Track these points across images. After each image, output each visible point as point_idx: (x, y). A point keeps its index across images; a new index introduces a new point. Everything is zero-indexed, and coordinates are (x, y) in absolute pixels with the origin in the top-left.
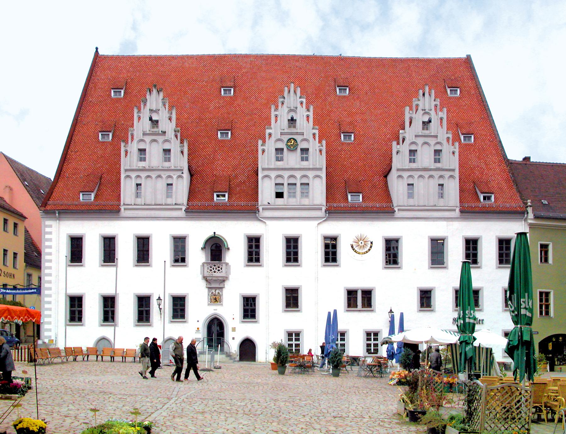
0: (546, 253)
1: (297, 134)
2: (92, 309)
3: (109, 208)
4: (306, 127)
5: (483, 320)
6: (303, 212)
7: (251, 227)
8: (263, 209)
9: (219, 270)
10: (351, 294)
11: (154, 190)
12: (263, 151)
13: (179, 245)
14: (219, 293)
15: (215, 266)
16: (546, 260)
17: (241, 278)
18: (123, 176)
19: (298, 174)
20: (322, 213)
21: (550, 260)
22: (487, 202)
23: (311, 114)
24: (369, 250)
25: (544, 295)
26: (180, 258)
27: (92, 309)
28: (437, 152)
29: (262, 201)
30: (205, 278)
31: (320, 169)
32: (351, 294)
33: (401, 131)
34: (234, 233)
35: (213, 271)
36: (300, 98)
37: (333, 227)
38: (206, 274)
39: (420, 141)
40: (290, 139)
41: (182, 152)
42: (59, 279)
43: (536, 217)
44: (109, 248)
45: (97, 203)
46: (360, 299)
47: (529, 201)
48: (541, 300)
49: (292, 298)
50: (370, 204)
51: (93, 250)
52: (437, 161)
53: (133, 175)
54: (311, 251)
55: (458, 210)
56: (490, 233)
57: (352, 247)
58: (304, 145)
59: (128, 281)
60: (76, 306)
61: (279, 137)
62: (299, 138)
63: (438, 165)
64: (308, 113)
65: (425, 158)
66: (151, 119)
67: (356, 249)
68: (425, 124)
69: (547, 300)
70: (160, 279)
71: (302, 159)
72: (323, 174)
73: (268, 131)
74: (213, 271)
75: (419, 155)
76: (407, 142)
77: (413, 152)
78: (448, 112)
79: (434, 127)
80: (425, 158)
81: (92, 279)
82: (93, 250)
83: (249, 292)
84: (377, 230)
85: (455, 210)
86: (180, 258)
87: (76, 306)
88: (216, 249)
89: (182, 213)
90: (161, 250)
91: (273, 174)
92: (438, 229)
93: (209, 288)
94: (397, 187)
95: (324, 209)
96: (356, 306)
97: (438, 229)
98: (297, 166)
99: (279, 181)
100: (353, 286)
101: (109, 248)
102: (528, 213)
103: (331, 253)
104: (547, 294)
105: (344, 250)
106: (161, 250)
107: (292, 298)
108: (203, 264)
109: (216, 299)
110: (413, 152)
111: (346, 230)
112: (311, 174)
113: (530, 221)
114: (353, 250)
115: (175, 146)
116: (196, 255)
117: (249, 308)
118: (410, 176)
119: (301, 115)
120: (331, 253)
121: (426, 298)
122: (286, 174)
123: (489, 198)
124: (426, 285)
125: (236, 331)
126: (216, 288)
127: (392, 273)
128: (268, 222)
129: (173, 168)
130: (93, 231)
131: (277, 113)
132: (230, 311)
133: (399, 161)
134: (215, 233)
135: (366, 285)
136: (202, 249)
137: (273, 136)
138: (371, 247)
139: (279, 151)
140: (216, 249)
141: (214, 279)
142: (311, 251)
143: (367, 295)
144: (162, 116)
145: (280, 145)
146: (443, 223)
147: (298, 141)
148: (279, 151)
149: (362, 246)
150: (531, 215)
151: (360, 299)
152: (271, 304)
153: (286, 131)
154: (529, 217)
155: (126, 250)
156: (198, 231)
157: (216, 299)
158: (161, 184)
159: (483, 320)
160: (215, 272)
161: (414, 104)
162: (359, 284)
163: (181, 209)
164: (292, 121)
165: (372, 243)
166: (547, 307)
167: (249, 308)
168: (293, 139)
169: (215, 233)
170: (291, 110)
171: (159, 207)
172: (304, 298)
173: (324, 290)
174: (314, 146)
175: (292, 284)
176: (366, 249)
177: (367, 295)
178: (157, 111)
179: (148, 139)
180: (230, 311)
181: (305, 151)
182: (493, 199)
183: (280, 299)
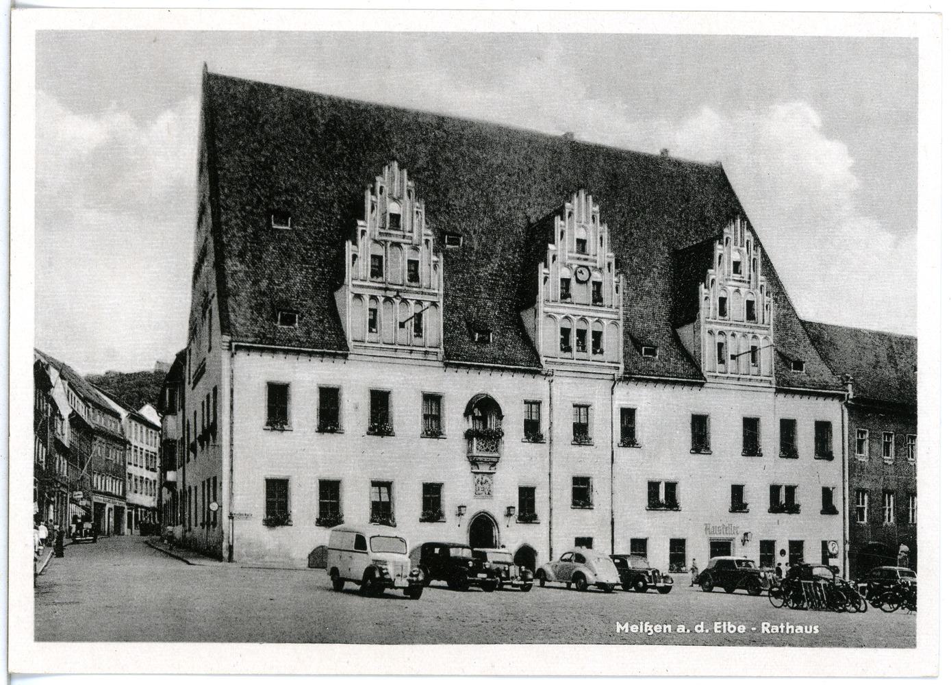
2: (304, 502)
3: (333, 344)
7: (535, 387)
12: (546, 279)
17: (518, 462)
26: (433, 427)
27: (304, 502)
32: (653, 487)
37: (629, 395)
41: (430, 265)
49: (582, 493)
51: (304, 408)
54: (604, 428)
56: (807, 412)
58: (596, 276)
59: (352, 458)
60: (277, 495)
70: (412, 459)
80: (736, 309)
81: (303, 455)
82: (304, 408)
86: (433, 427)
87: (277, 495)
100: (656, 479)
107: (582, 493)
109: (483, 488)
116: (455, 422)
125: (511, 536)
135: (671, 478)
139: (566, 283)
142: (604, 428)
143: (671, 487)
145: (566, 273)
148: (566, 283)
151: (663, 497)
152: (554, 499)
157: (483, 488)
162: (664, 474)
171: (393, 346)
172: (599, 495)
173: (623, 479)
174: (610, 280)
183: (565, 493)
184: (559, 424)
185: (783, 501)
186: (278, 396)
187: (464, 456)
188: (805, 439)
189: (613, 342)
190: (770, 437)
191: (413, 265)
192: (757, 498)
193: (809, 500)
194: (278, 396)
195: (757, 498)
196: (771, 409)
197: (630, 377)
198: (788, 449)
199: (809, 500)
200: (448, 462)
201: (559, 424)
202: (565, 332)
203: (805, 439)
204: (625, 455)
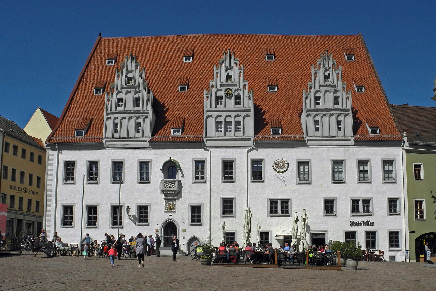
0: (419, 171)
1: (233, 85)
4: (238, 78)
5: (373, 223)
6: (236, 142)
8: (207, 140)
9: (173, 186)
10: (273, 203)
11: (127, 126)
12: (207, 98)
13: (144, 167)
14: (173, 203)
15: (170, 182)
16: (418, 176)
18: (105, 118)
19: (233, 114)
20: (251, 143)
21: (422, 177)
22: (375, 135)
23: (242, 71)
24: (287, 170)
25: (419, 202)
28: (336, 98)
29: (206, 135)
30: (163, 192)
31: (249, 111)
32: (273, 203)
33: (309, 83)
34: (185, 158)
35: (168, 186)
36: (234, 59)
38: (164, 189)
39: (323, 89)
40: (227, 89)
42: (59, 193)
43: (411, 145)
44: (93, 170)
45: (86, 137)
46: (279, 207)
47: (405, 133)
48: (416, 207)
49: (228, 207)
50: (287, 136)
51: (81, 171)
52: (336, 103)
53: (113, 116)
54: (242, 170)
55: (352, 139)
57: (274, 167)
61: (218, 87)
62: (233, 89)
63: (336, 107)
64: (240, 71)
65: (328, 101)
66: (126, 76)
67: (277, 169)
68: (327, 78)
69: (421, 207)
71: (236, 103)
72: (251, 113)
73: (211, 84)
74: (168, 186)
75: (321, 101)
76: (313, 91)
77: (318, 98)
78: (342, 69)
79: (334, 79)
80: (328, 101)
83: (196, 202)
84: (292, 155)
85: (350, 140)
88: (171, 169)
89: (147, 144)
90: (131, 172)
91: (215, 114)
92: (337, 154)
93: (165, 199)
94: (307, 123)
95: (252, 139)
96: (276, 212)
97: (337, 154)
98: (233, 109)
99: (219, 119)
101: (93, 170)
102: (404, 142)
103: (257, 173)
104: (421, 202)
105: (268, 170)
106: (131, 172)
107: (228, 207)
108: (162, 180)
110: (318, 98)
111: (269, 155)
112: (243, 114)
113: (406, 148)
114: (275, 169)
115: (143, 95)
116: (157, 175)
117: (196, 214)
118: (316, 115)
119: (235, 72)
120: (257, 173)
121: (329, 206)
122: (224, 114)
123: (376, 131)
124: (330, 196)
125: (186, 232)
126: (171, 200)
127: (304, 187)
128: (210, 150)
129: (141, 111)
130: (81, 158)
131: (217, 71)
132: (181, 216)
133: (309, 103)
134: (170, 158)
136: (161, 170)
137: (214, 87)
138: (288, 168)
139: (219, 98)
140: (171, 169)
141: (169, 192)
142: (242, 170)
143: (285, 203)
144: (135, 75)
146: (342, 149)
147: (233, 90)
148: (219, 98)
149: (281, 167)
150: (407, 143)
151: (279, 207)
152: (212, 212)
153: (224, 83)
154: (405, 145)
155: (105, 172)
156: (158, 158)
158: (133, 122)
159: (373, 223)
160: (170, 187)
161: (318, 63)
162: (279, 196)
163: (146, 141)
164: (228, 77)
165: (288, 164)
166: (421, 212)
167: (196, 214)
168: (229, 89)
169: (170, 158)
170: (227, 69)
174: (244, 94)
175: (228, 196)
176: (284, 170)
177: (285, 203)
178: (131, 71)
179: (124, 91)
180: (181, 216)
181: (238, 98)
182: (378, 132)
183: (218, 207)
184: (214, 170)
185: (361, 206)
186: (70, 167)
187: (160, 191)
188: (376, 170)
189: (249, 125)
190: (351, 170)
191: (137, 100)
192: (343, 207)
193: (380, 207)
194: (70, 167)
195: (343, 207)
196: (352, 155)
197: (259, 144)
198: (363, 176)
199: (380, 207)
200: (152, 194)
201: (214, 170)
202: (218, 123)
203: (376, 170)
204: (255, 187)
